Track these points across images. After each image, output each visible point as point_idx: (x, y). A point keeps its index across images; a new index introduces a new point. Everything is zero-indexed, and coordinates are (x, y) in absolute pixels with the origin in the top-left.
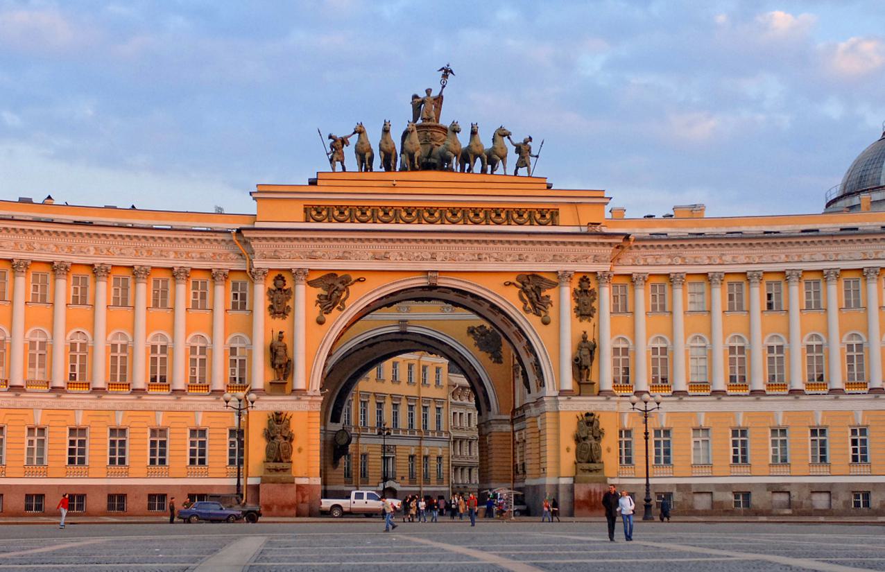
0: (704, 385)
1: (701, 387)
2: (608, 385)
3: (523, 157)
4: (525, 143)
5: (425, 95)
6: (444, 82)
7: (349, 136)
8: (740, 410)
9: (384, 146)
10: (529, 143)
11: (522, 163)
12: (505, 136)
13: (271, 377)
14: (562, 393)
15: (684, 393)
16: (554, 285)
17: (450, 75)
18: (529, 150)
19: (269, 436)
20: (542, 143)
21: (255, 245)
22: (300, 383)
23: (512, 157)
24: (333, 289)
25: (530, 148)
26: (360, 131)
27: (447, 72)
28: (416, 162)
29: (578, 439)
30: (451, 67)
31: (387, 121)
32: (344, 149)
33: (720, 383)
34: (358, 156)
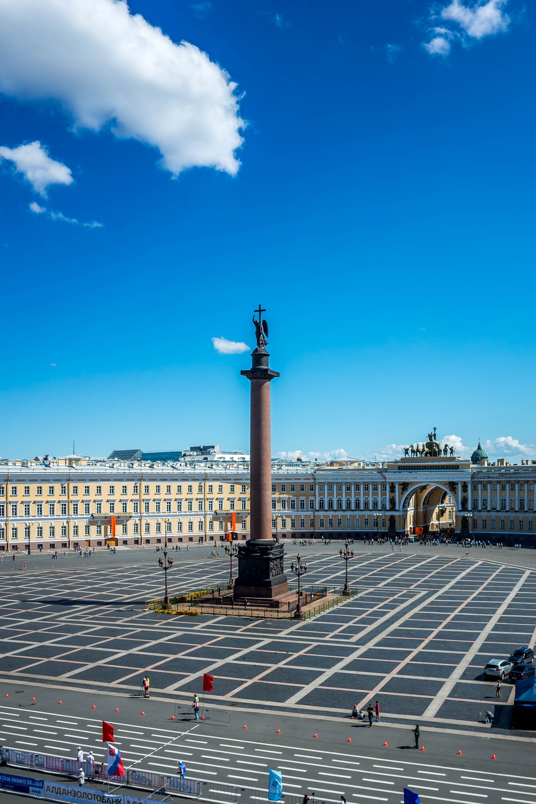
0: (495, 509)
1: (494, 509)
2: (470, 509)
8: (503, 514)
11: (451, 453)
13: (391, 507)
14: (459, 511)
15: (490, 511)
16: (457, 484)
19: (390, 520)
21: (386, 476)
22: (397, 508)
23: (449, 451)
24: (405, 486)
26: (412, 446)
27: (435, 429)
29: (462, 522)
33: (498, 509)
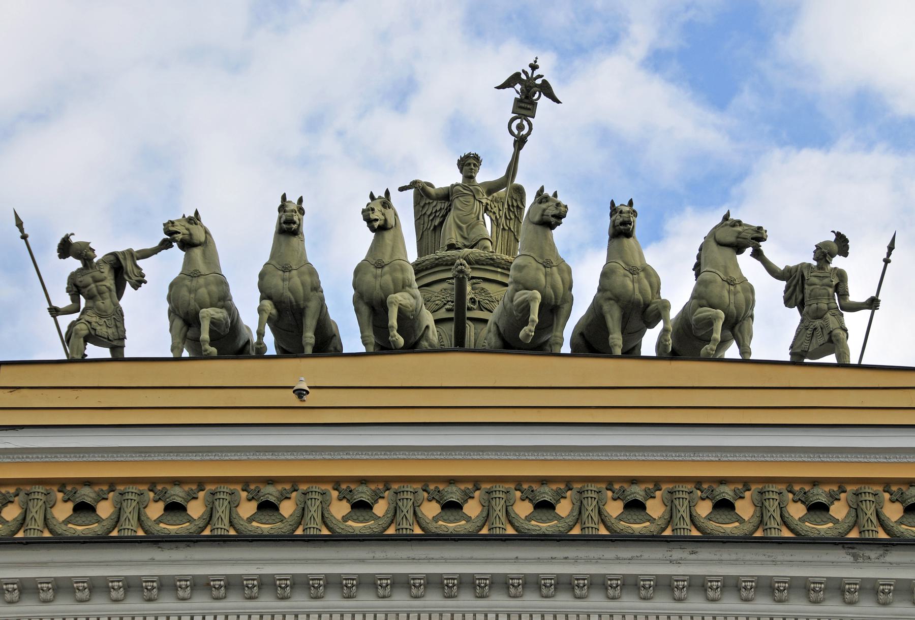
3: (819, 315)
4: (823, 254)
5: (456, 177)
6: (520, 127)
7: (146, 254)
9: (277, 282)
10: (837, 262)
12: (739, 250)
17: (543, 102)
18: (844, 295)
20: (891, 248)
25: (842, 276)
27: (529, 92)
28: (393, 321)
30: (546, 71)
31: (293, 198)
32: (122, 303)
34: (179, 323)
